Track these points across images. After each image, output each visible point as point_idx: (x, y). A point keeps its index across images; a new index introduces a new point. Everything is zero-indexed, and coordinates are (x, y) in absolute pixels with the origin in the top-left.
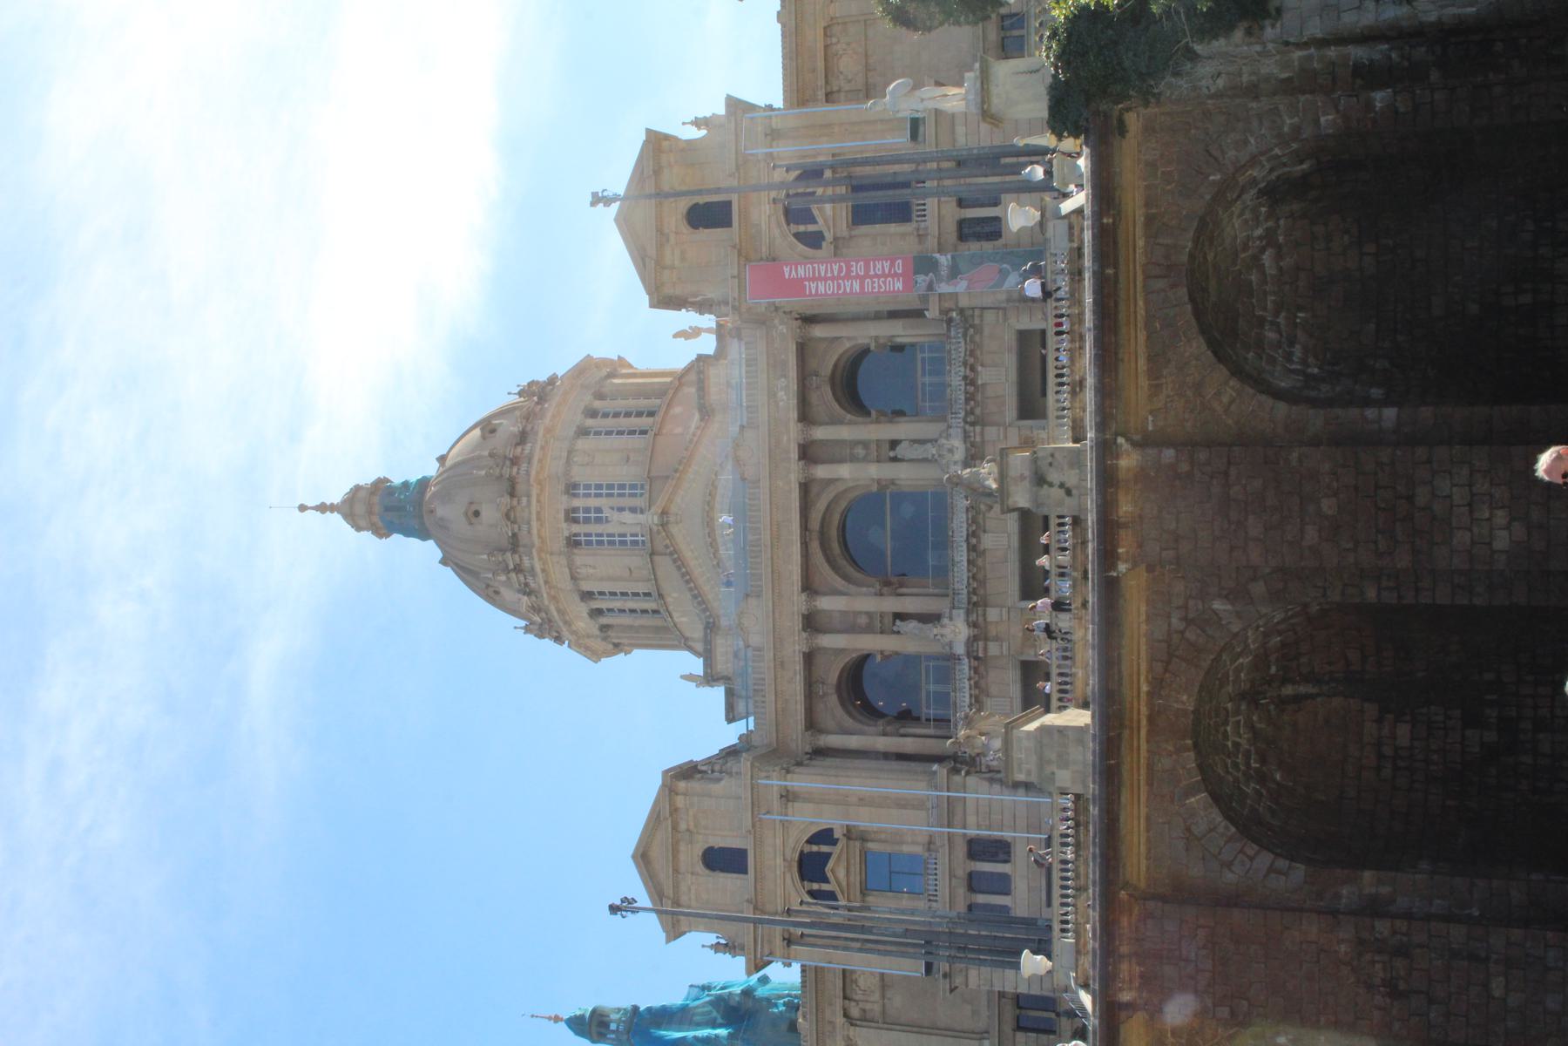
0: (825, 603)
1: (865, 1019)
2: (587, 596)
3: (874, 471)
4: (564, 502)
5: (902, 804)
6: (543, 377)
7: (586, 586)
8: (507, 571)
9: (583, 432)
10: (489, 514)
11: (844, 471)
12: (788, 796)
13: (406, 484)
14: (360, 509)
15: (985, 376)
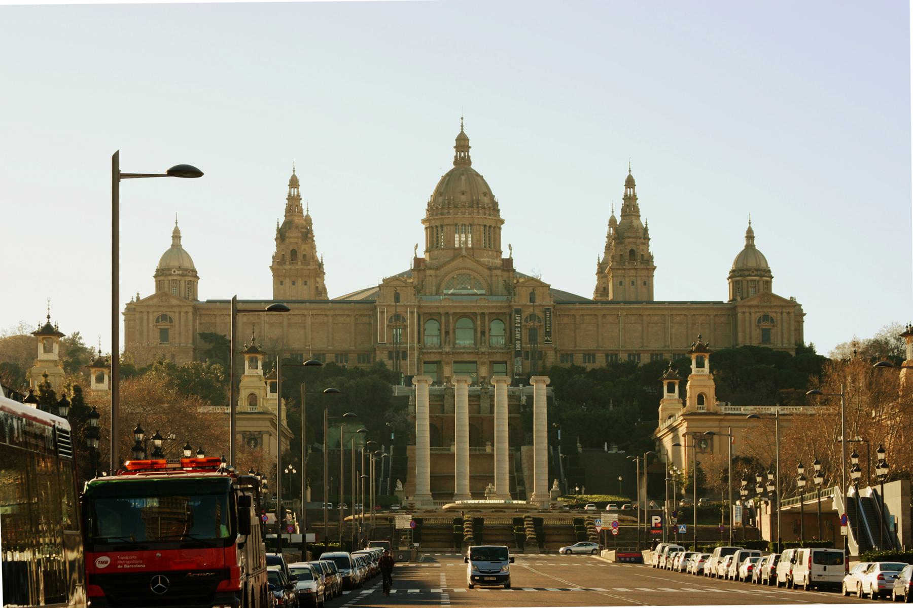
0: (451, 318)
1: (356, 319)
2: (442, 226)
3: (479, 329)
4: (467, 223)
5: (412, 337)
6: (499, 207)
7: (444, 228)
8: (449, 204)
9: (485, 226)
10: (463, 198)
11: (479, 322)
12: (412, 313)
13: (469, 157)
14: (462, 143)
15: (498, 355)
